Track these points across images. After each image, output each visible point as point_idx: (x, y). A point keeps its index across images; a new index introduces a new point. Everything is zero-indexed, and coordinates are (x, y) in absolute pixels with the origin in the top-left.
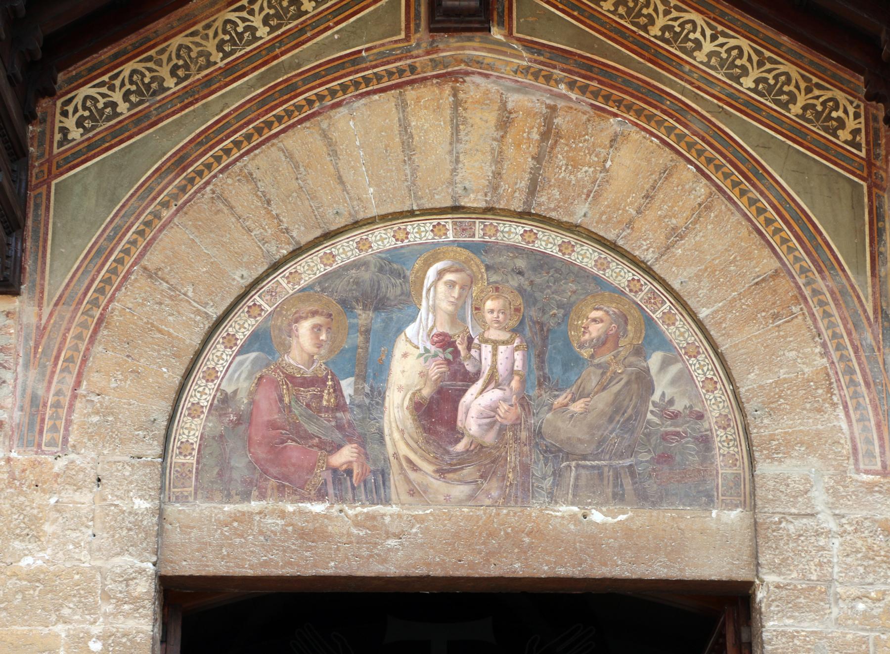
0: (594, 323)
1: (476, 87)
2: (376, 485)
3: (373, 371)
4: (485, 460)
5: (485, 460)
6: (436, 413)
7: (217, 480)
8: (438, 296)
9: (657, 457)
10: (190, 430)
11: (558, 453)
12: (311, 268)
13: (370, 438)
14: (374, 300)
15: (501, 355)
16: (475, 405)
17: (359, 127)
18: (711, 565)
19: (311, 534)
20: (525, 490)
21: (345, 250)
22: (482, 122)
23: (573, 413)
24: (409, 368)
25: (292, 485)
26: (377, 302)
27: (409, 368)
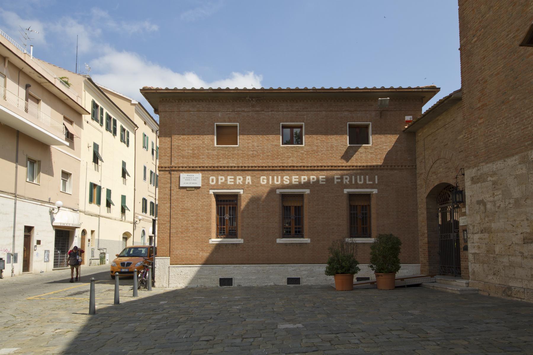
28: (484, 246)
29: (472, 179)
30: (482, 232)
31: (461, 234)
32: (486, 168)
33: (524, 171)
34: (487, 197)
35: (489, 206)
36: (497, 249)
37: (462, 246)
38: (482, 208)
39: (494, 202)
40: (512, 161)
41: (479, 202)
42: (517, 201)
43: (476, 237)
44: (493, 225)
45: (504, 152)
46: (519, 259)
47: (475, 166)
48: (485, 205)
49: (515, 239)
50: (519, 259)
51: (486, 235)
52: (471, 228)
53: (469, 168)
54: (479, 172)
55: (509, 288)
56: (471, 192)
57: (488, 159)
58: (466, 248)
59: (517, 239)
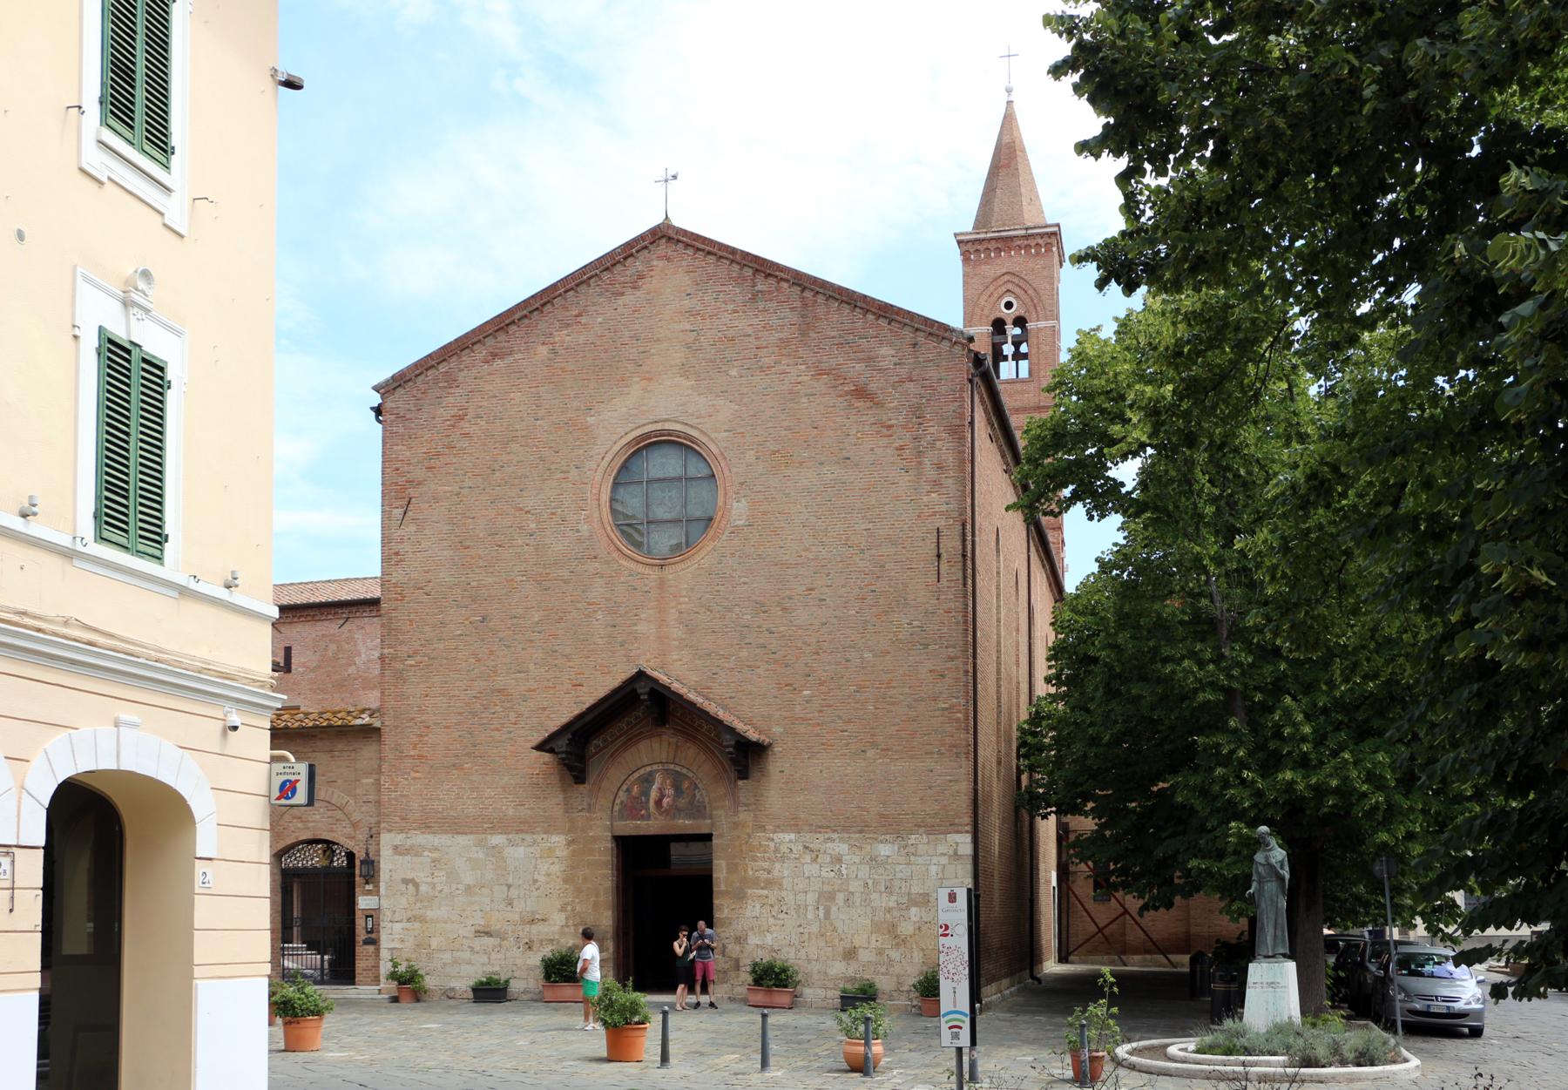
0: (686, 784)
1: (664, 737)
2: (649, 818)
3: (647, 795)
4: (667, 812)
5: (667, 812)
6: (659, 803)
7: (621, 817)
8: (658, 779)
9: (697, 810)
10: (617, 808)
11: (679, 810)
12: (636, 775)
13: (647, 809)
14: (647, 780)
15: (670, 791)
16: (666, 801)
17: (643, 746)
18: (705, 831)
19: (638, 827)
20: (674, 818)
21: (642, 771)
22: (665, 745)
23: (683, 802)
24: (654, 794)
25: (634, 818)
26: (647, 781)
27: (654, 794)
28: (411, 940)
29: (396, 848)
30: (408, 920)
31: (360, 922)
32: (420, 839)
33: (481, 855)
34: (421, 876)
35: (423, 888)
36: (434, 943)
37: (361, 935)
38: (410, 886)
39: (434, 886)
40: (462, 840)
41: (406, 882)
42: (468, 888)
43: (398, 926)
44: (429, 913)
45: (454, 826)
46: (467, 955)
47: (402, 831)
48: (416, 885)
49: (462, 932)
50: (467, 955)
51: (417, 925)
52: (388, 913)
53: (390, 831)
54: (409, 842)
55: (453, 989)
56: (388, 865)
57: (426, 826)
58: (373, 942)
59: (468, 931)
